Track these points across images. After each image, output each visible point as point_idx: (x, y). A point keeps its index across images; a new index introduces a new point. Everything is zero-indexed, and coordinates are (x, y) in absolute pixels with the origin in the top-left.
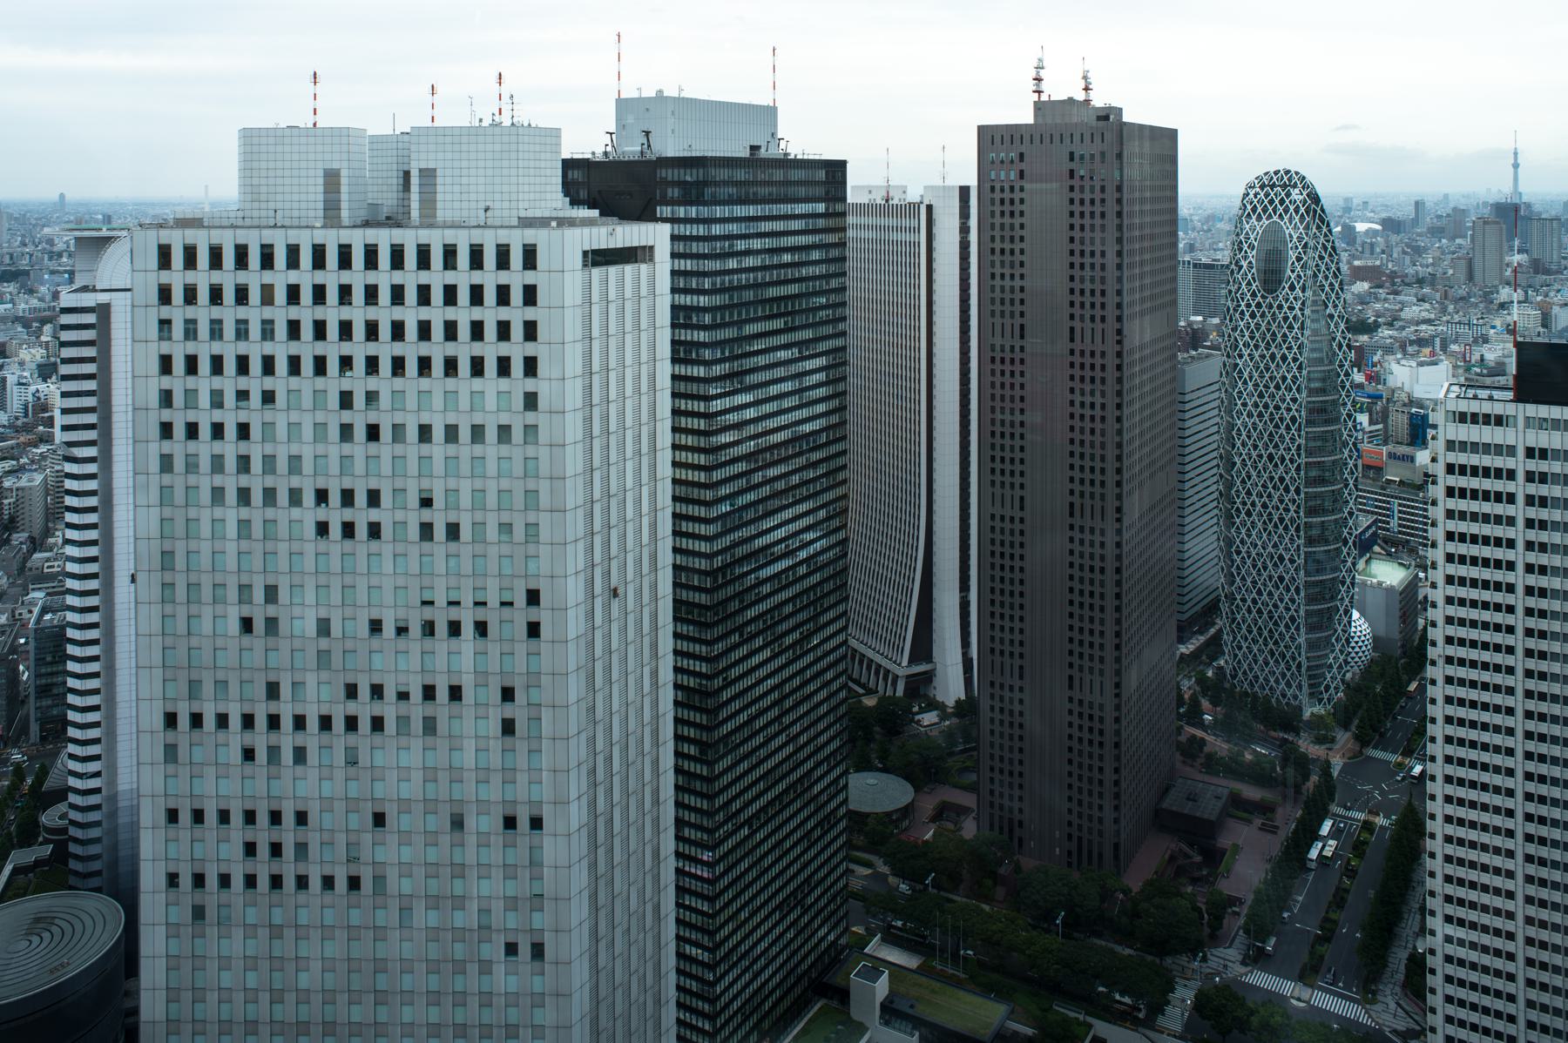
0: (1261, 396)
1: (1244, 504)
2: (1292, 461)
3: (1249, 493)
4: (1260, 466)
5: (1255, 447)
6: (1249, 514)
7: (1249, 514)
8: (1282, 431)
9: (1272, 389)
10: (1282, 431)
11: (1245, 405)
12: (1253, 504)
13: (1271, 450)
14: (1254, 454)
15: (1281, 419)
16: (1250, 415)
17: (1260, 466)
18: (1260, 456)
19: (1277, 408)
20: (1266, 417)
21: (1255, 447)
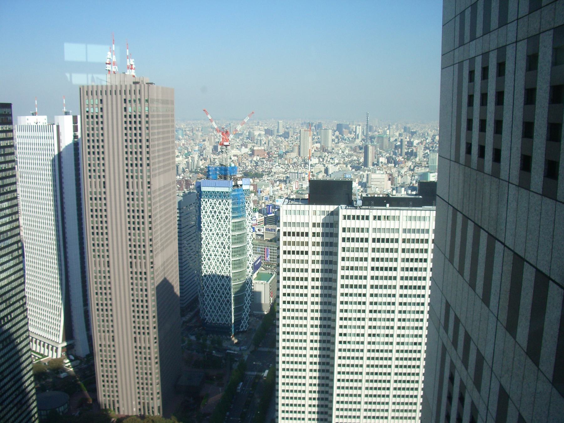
0: (213, 208)
1: (207, 255)
2: (226, 235)
3: (209, 250)
4: (213, 238)
5: (211, 230)
6: (209, 259)
7: (209, 259)
8: (222, 222)
9: (218, 205)
10: (222, 222)
11: (206, 212)
12: (211, 255)
13: (217, 231)
14: (211, 233)
15: (221, 217)
16: (208, 217)
17: (213, 238)
18: (213, 234)
19: (220, 213)
20: (216, 217)
21: (211, 230)
